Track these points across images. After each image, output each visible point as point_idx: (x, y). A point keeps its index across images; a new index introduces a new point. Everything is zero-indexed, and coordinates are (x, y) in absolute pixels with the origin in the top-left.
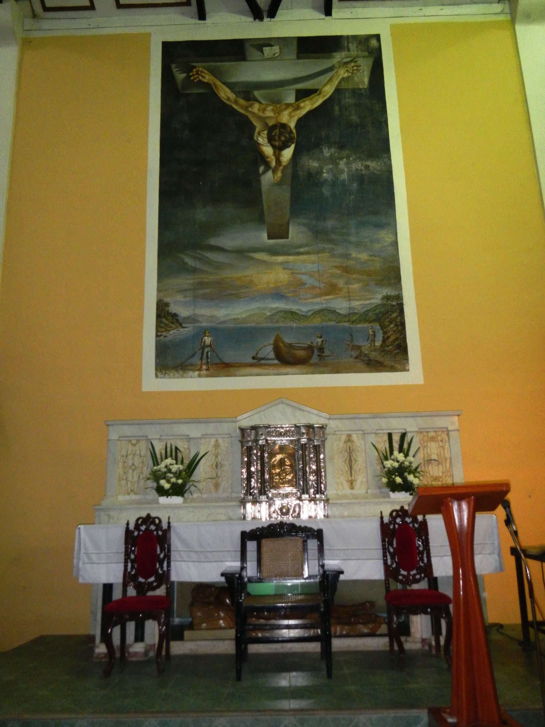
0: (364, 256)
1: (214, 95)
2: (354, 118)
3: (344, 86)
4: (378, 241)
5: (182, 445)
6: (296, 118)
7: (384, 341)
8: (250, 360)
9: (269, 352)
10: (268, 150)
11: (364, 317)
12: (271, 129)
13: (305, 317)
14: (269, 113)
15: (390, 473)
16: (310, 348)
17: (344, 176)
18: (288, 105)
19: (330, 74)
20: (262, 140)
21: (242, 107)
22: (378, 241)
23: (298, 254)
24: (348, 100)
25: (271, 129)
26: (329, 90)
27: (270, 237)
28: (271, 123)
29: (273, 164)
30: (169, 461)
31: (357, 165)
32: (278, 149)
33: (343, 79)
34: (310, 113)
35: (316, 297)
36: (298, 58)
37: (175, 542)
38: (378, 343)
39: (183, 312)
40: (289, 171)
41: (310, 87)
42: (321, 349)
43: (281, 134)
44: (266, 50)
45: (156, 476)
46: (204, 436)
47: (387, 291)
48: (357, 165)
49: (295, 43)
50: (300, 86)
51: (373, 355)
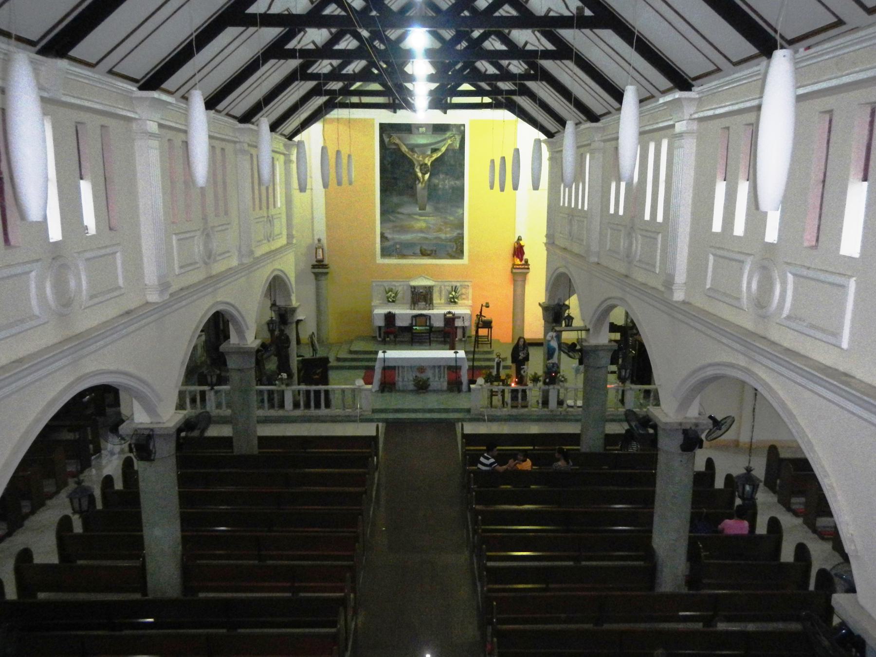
0: (452, 218)
1: (399, 149)
2: (452, 162)
3: (449, 148)
4: (457, 213)
5: (394, 288)
6: (430, 161)
7: (456, 249)
8: (412, 254)
9: (418, 251)
10: (420, 175)
11: (450, 240)
12: (421, 165)
13: (431, 240)
14: (421, 159)
15: (451, 298)
16: (432, 251)
17: (447, 187)
18: (428, 156)
19: (445, 142)
20: (418, 170)
21: (411, 155)
22: (457, 213)
23: (429, 216)
24: (450, 154)
25: (421, 165)
26: (443, 149)
27: (420, 209)
28: (421, 163)
29: (422, 180)
30: (390, 293)
31: (452, 183)
32: (424, 174)
33: (449, 144)
34: (436, 160)
35: (434, 232)
36: (433, 134)
37: (396, 317)
38: (454, 250)
39: (389, 236)
40: (427, 183)
41: (437, 147)
42: (435, 251)
43: (425, 168)
44: (420, 129)
45: (388, 298)
46: (400, 285)
47: (459, 231)
48: (452, 183)
49: (432, 127)
50: (433, 147)
51: (453, 254)
